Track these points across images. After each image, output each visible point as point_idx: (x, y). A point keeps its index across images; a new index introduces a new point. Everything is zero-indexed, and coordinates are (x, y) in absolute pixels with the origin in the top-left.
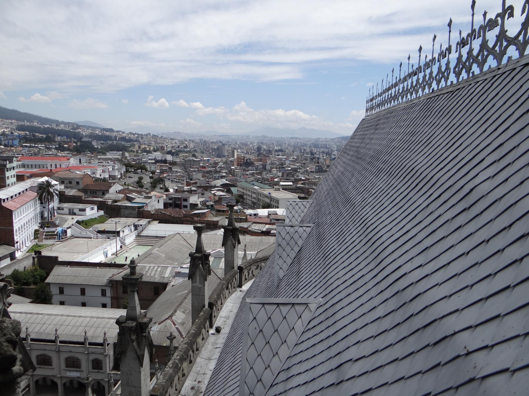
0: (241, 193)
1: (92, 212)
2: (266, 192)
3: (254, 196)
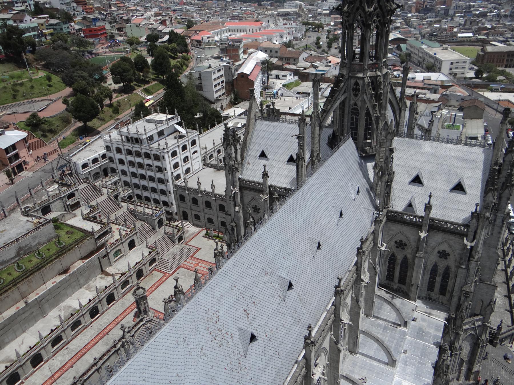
0: (408, 52)
1: (291, 78)
2: (432, 53)
3: (421, 55)
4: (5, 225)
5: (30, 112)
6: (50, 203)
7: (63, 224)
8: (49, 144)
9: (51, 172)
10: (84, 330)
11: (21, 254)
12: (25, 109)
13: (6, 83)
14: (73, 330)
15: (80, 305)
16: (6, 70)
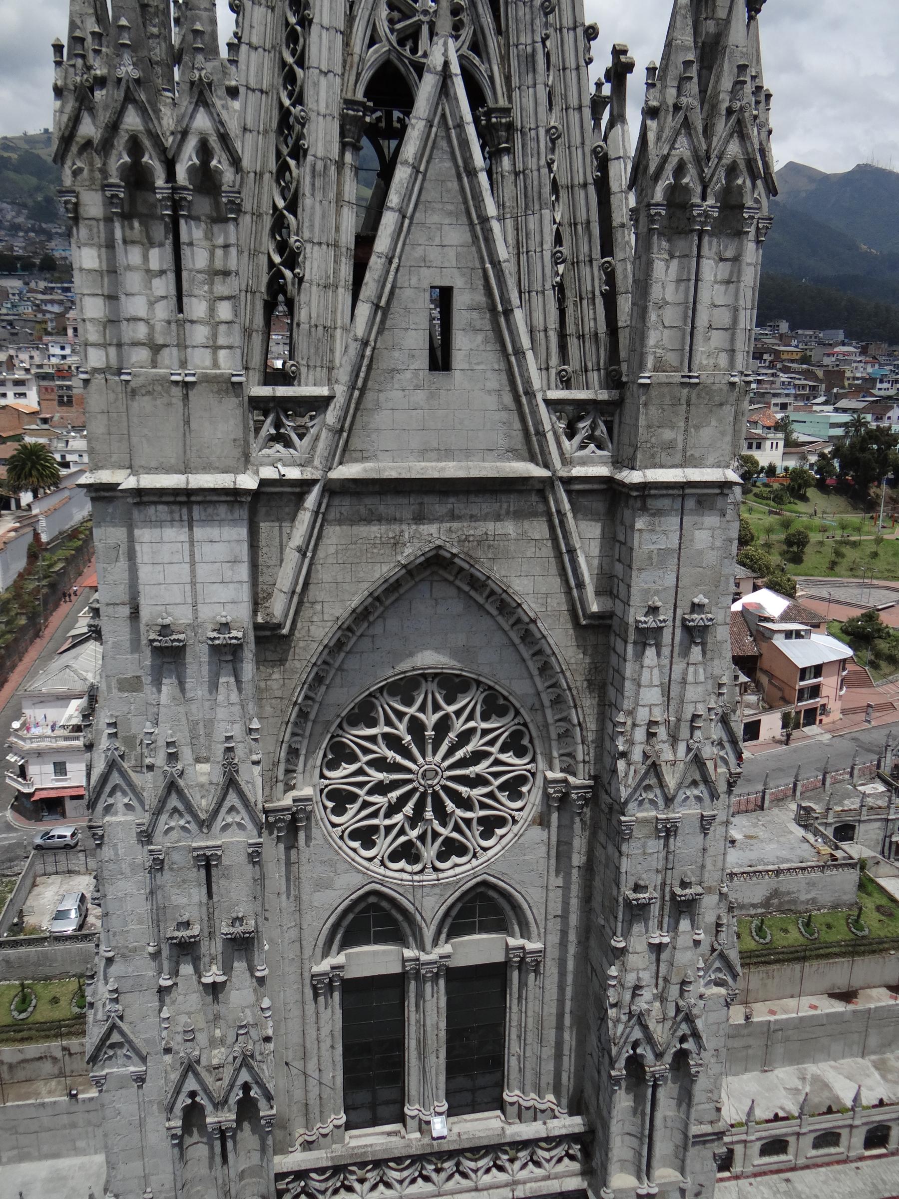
4: (755, 825)
5: (860, 607)
6: (859, 821)
7: (872, 881)
8: (878, 686)
9: (879, 753)
10: (838, 1162)
11: (772, 905)
12: (853, 597)
13: (827, 534)
14: (817, 1145)
15: (856, 1099)
16: (828, 510)
